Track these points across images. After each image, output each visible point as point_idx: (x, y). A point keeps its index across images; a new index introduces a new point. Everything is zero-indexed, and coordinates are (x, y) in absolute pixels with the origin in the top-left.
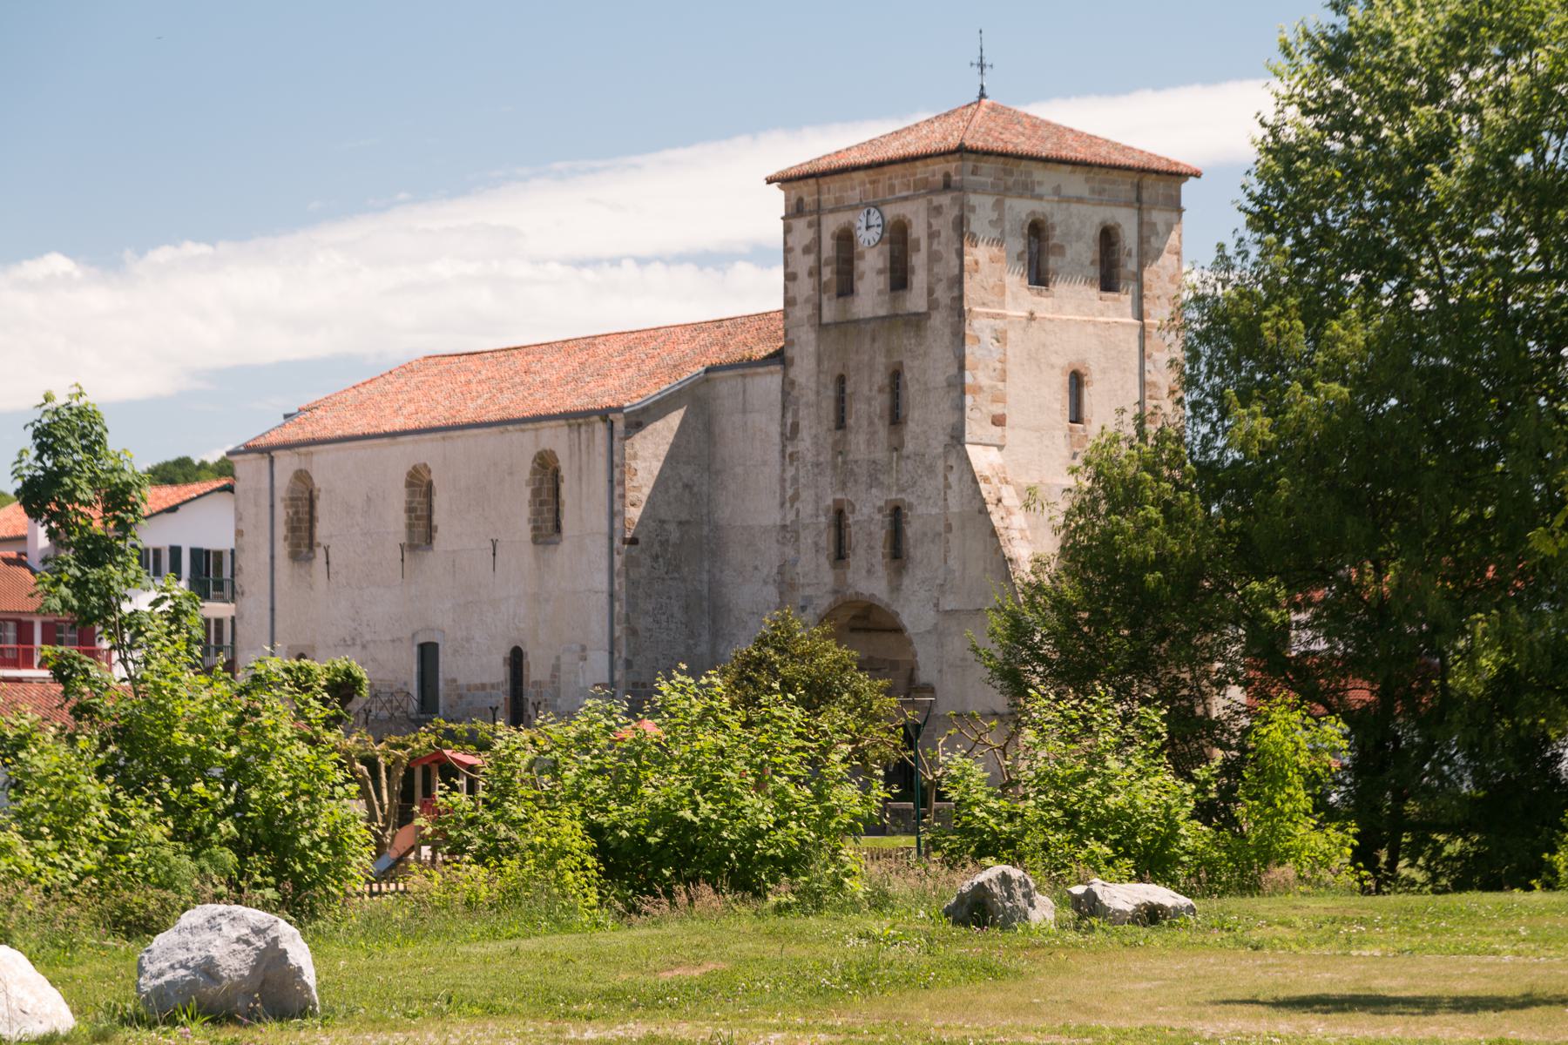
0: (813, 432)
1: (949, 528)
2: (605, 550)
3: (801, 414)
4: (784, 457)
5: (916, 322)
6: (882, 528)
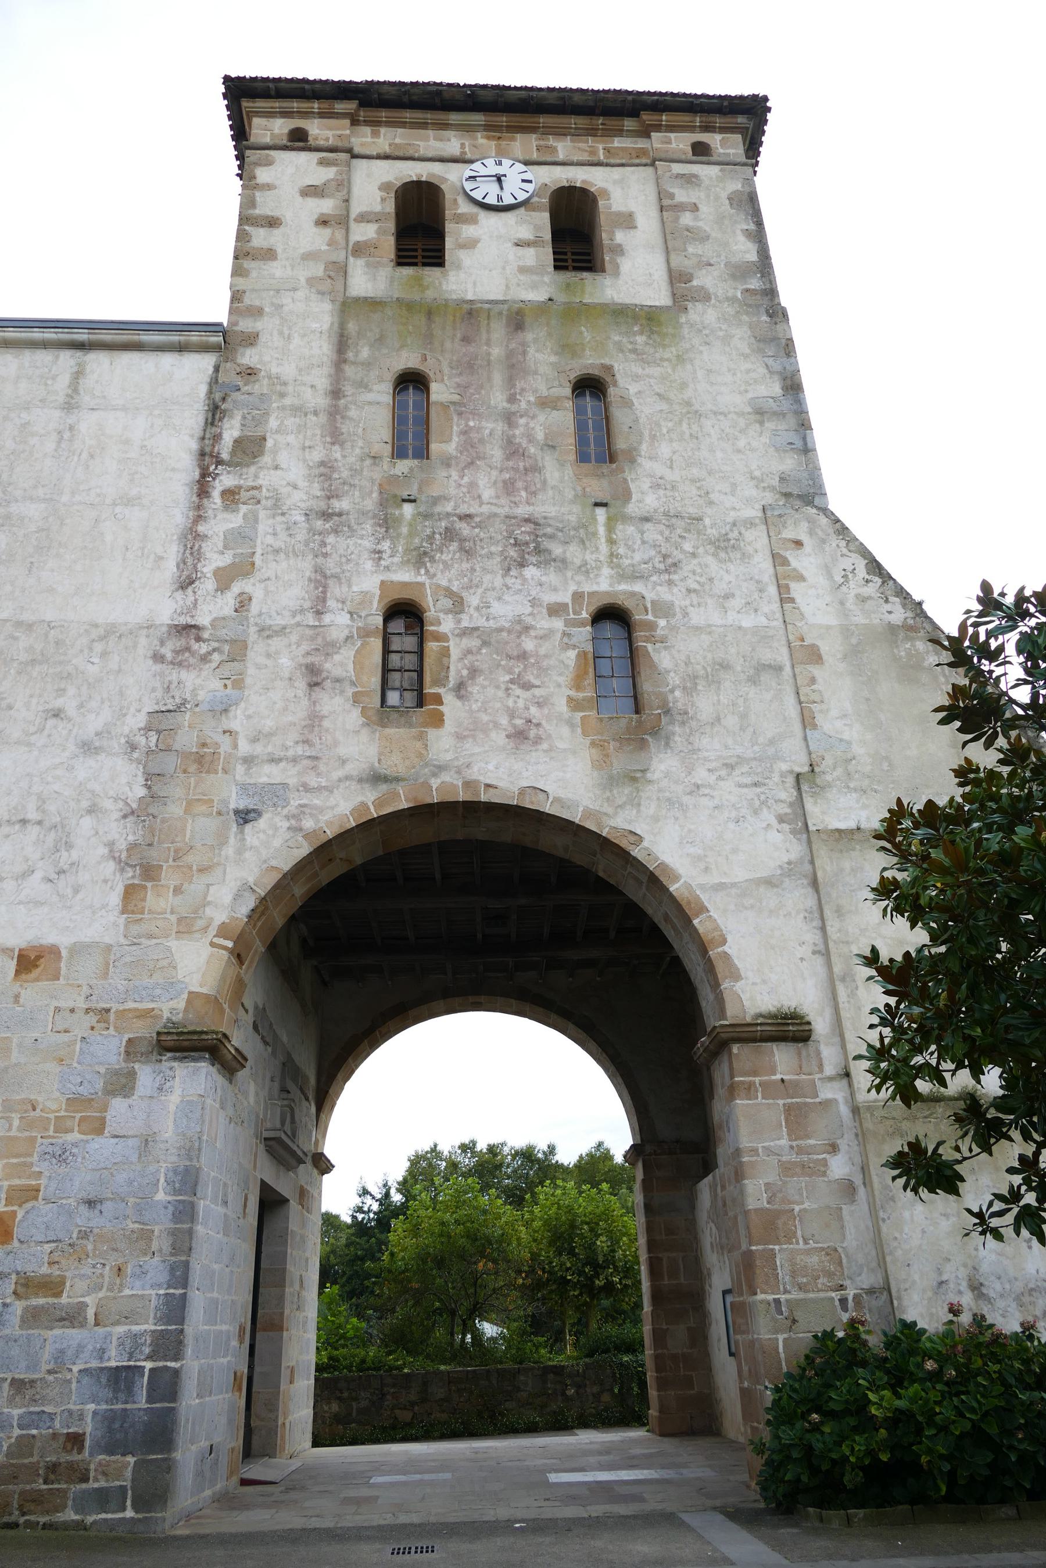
0: (317, 455)
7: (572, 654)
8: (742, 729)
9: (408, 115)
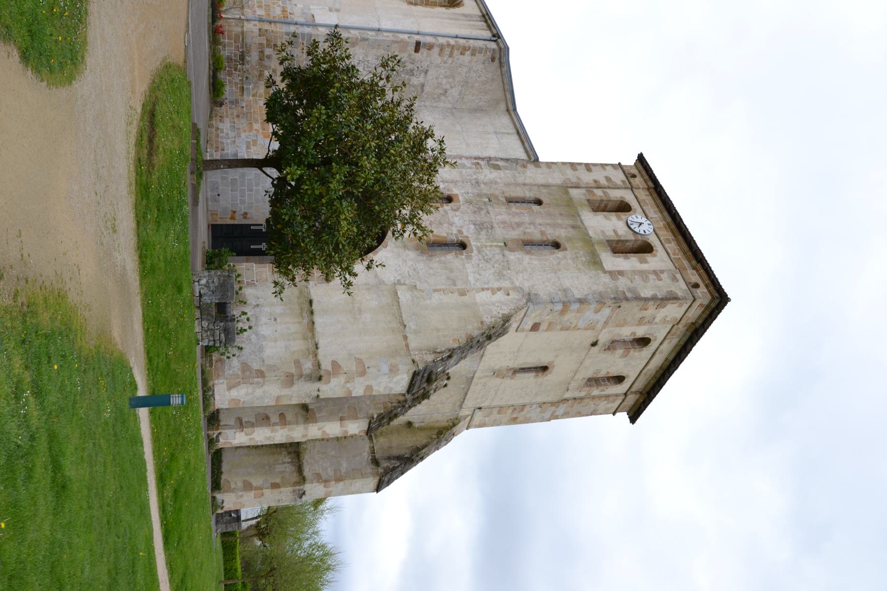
0: (499, 180)
1: (463, 293)
2: (409, 29)
3: (507, 172)
4: (476, 158)
5: (595, 262)
6: (448, 234)
7: (445, 235)
8: (429, 274)
9: (659, 201)
